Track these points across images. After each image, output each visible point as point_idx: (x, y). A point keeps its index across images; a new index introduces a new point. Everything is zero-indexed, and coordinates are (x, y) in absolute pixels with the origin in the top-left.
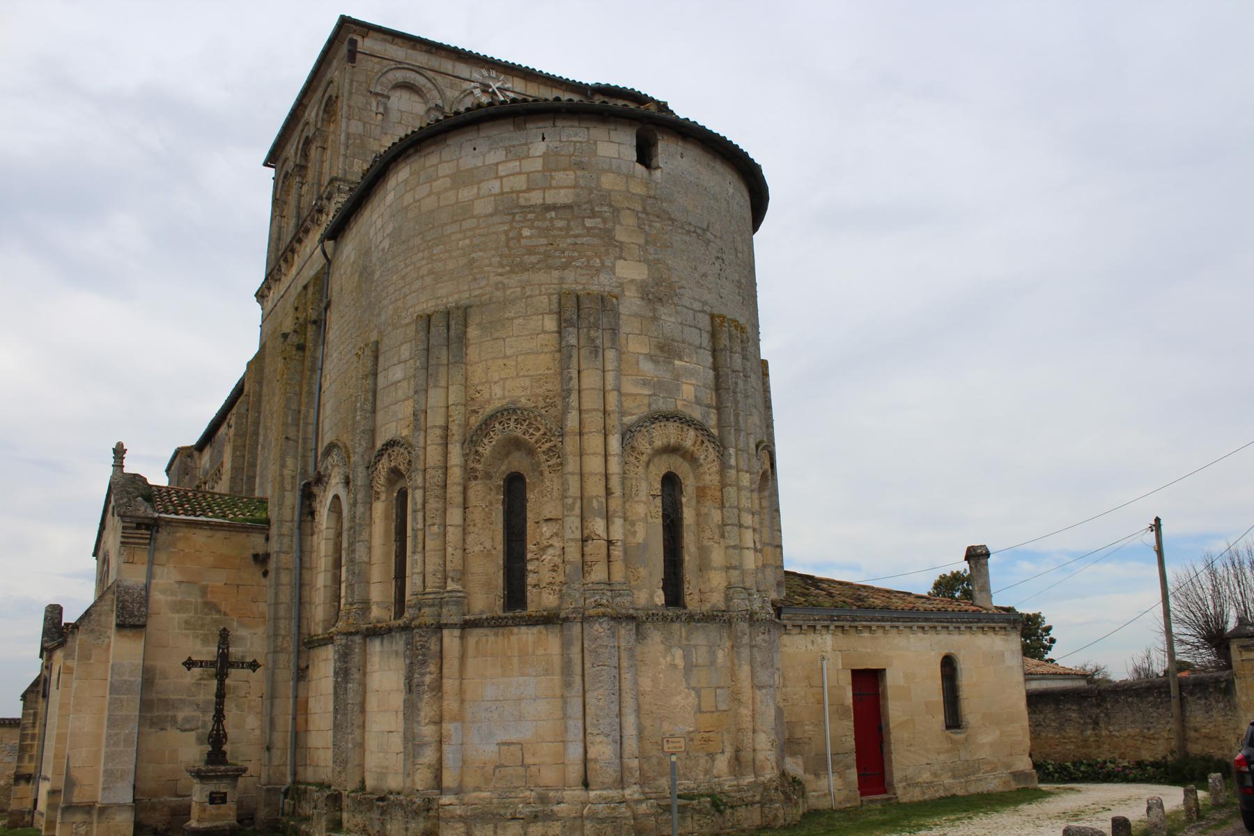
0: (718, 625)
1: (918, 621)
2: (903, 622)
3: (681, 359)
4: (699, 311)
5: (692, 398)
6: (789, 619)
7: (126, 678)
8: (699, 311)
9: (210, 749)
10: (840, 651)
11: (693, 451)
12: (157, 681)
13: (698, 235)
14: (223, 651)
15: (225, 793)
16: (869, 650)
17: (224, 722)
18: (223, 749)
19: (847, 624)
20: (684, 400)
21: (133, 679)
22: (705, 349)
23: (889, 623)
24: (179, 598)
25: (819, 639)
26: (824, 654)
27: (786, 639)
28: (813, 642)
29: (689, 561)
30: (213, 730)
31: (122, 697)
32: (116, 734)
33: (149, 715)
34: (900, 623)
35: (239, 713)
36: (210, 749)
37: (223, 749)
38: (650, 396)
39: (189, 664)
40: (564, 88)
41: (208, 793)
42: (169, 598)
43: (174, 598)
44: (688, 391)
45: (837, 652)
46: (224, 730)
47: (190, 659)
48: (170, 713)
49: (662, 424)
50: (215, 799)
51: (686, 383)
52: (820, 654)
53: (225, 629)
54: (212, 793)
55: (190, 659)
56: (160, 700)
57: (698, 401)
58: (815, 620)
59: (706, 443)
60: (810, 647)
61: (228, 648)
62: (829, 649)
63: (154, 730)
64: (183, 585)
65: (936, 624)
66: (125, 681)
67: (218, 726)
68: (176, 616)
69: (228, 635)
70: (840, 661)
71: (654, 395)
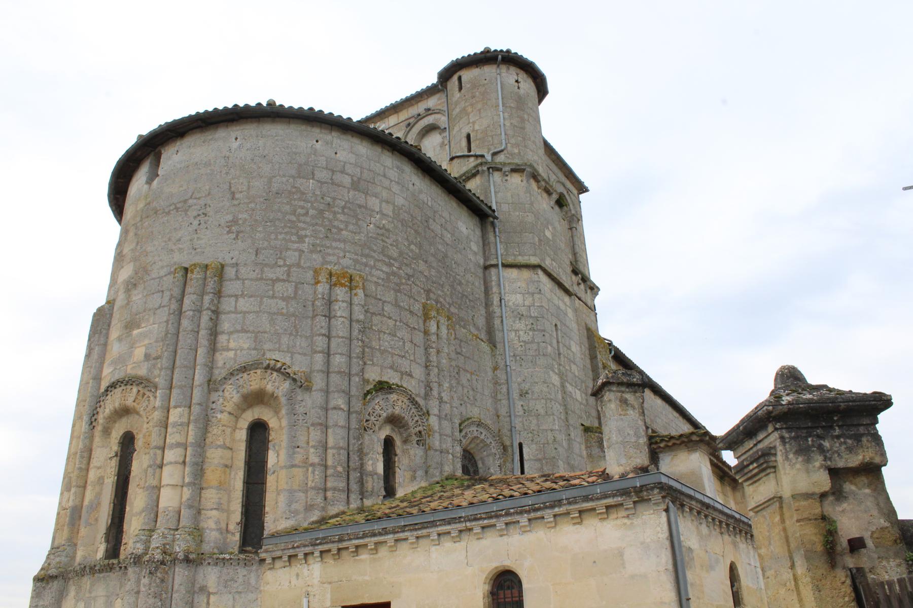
0: (120, 573)
1: (436, 526)
2: (411, 530)
3: (139, 327)
4: (165, 276)
5: (142, 357)
6: (266, 551)
8: (165, 276)
10: (330, 583)
11: (134, 406)
13: (177, 209)
16: (367, 578)
19: (334, 547)
20: (134, 363)
22: (164, 306)
23: (391, 536)
25: (304, 570)
26: (309, 589)
27: (269, 575)
28: (298, 575)
29: (128, 511)
34: (406, 534)
38: (112, 372)
40: (426, 97)
44: (139, 353)
45: (326, 585)
49: (112, 393)
51: (139, 347)
52: (304, 590)
57: (147, 357)
58: (293, 548)
59: (148, 393)
60: (294, 581)
62: (316, 581)
65: (468, 524)
70: (329, 596)
71: (115, 369)
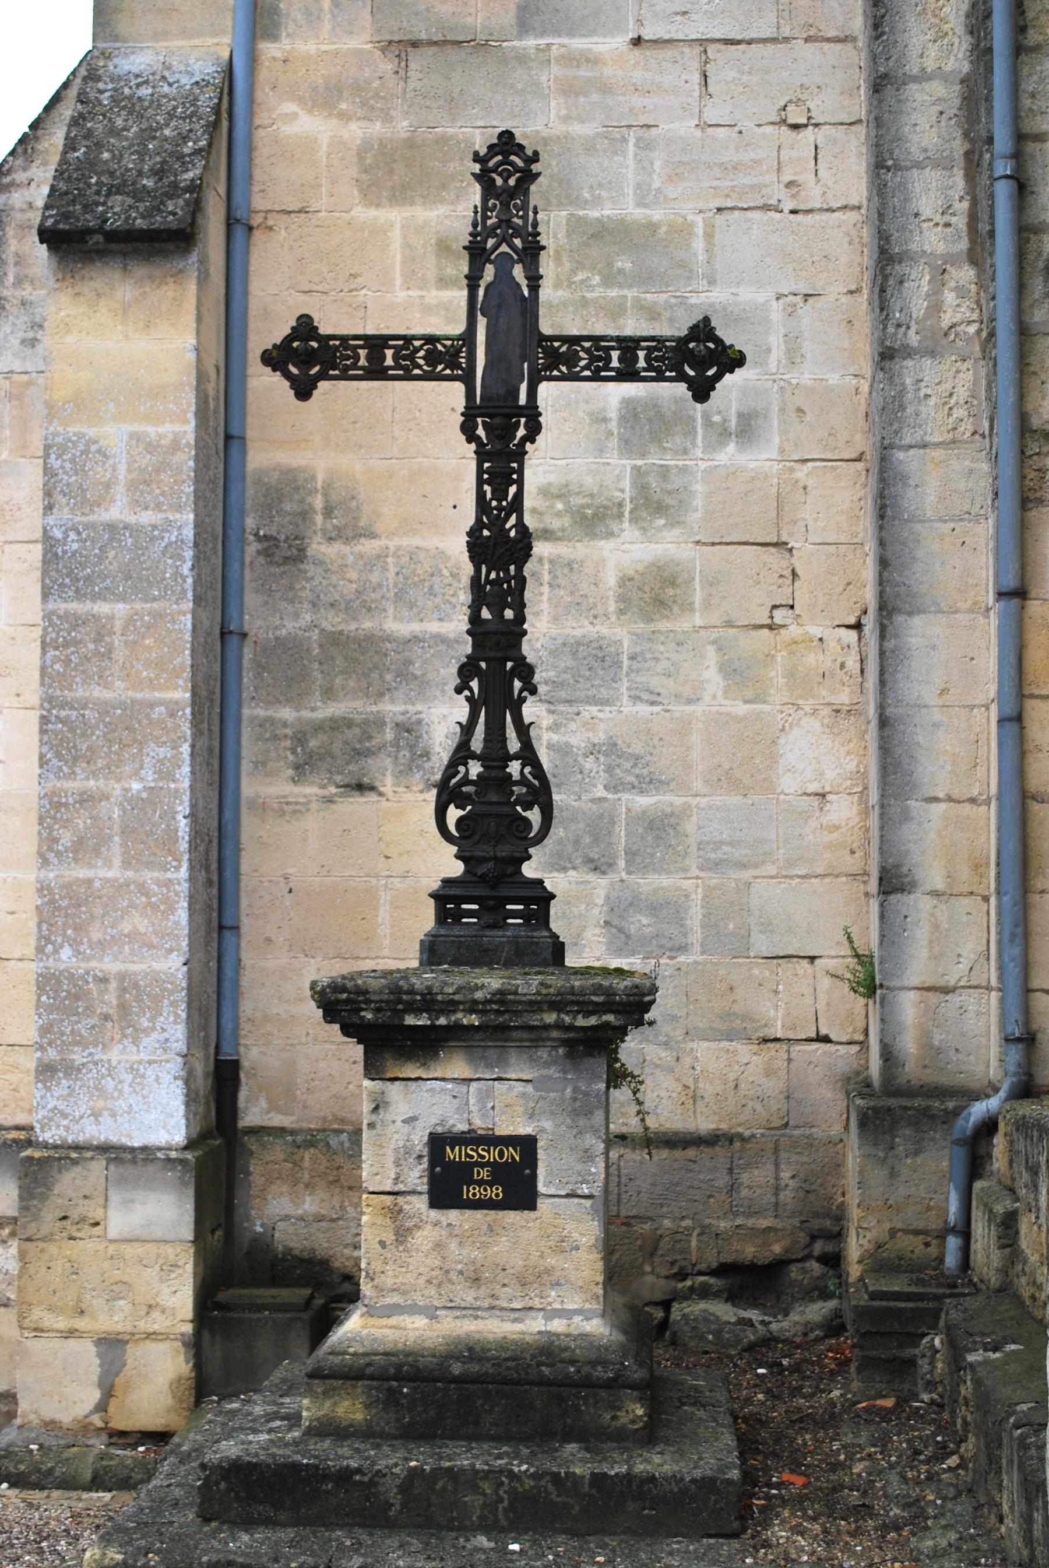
7: (116, 511)
9: (457, 869)
12: (318, 547)
14: (504, 274)
15: (527, 1145)
17: (530, 710)
18: (529, 870)
21: (147, 518)
24: (402, 126)
30: (462, 754)
31: (102, 608)
32: (86, 799)
33: (286, 713)
35: (742, 709)
36: (457, 869)
37: (529, 870)
39: (306, 359)
41: (419, 1139)
42: (356, 131)
43: (377, 129)
46: (528, 755)
47: (305, 327)
48: (392, 708)
50: (463, 1172)
53: (506, 143)
54: (438, 1142)
55: (305, 327)
56: (334, 640)
61: (532, 252)
63: (310, 790)
64: (417, 60)
66: (112, 528)
67: (495, 734)
68: (393, 216)
69: (528, 177)
